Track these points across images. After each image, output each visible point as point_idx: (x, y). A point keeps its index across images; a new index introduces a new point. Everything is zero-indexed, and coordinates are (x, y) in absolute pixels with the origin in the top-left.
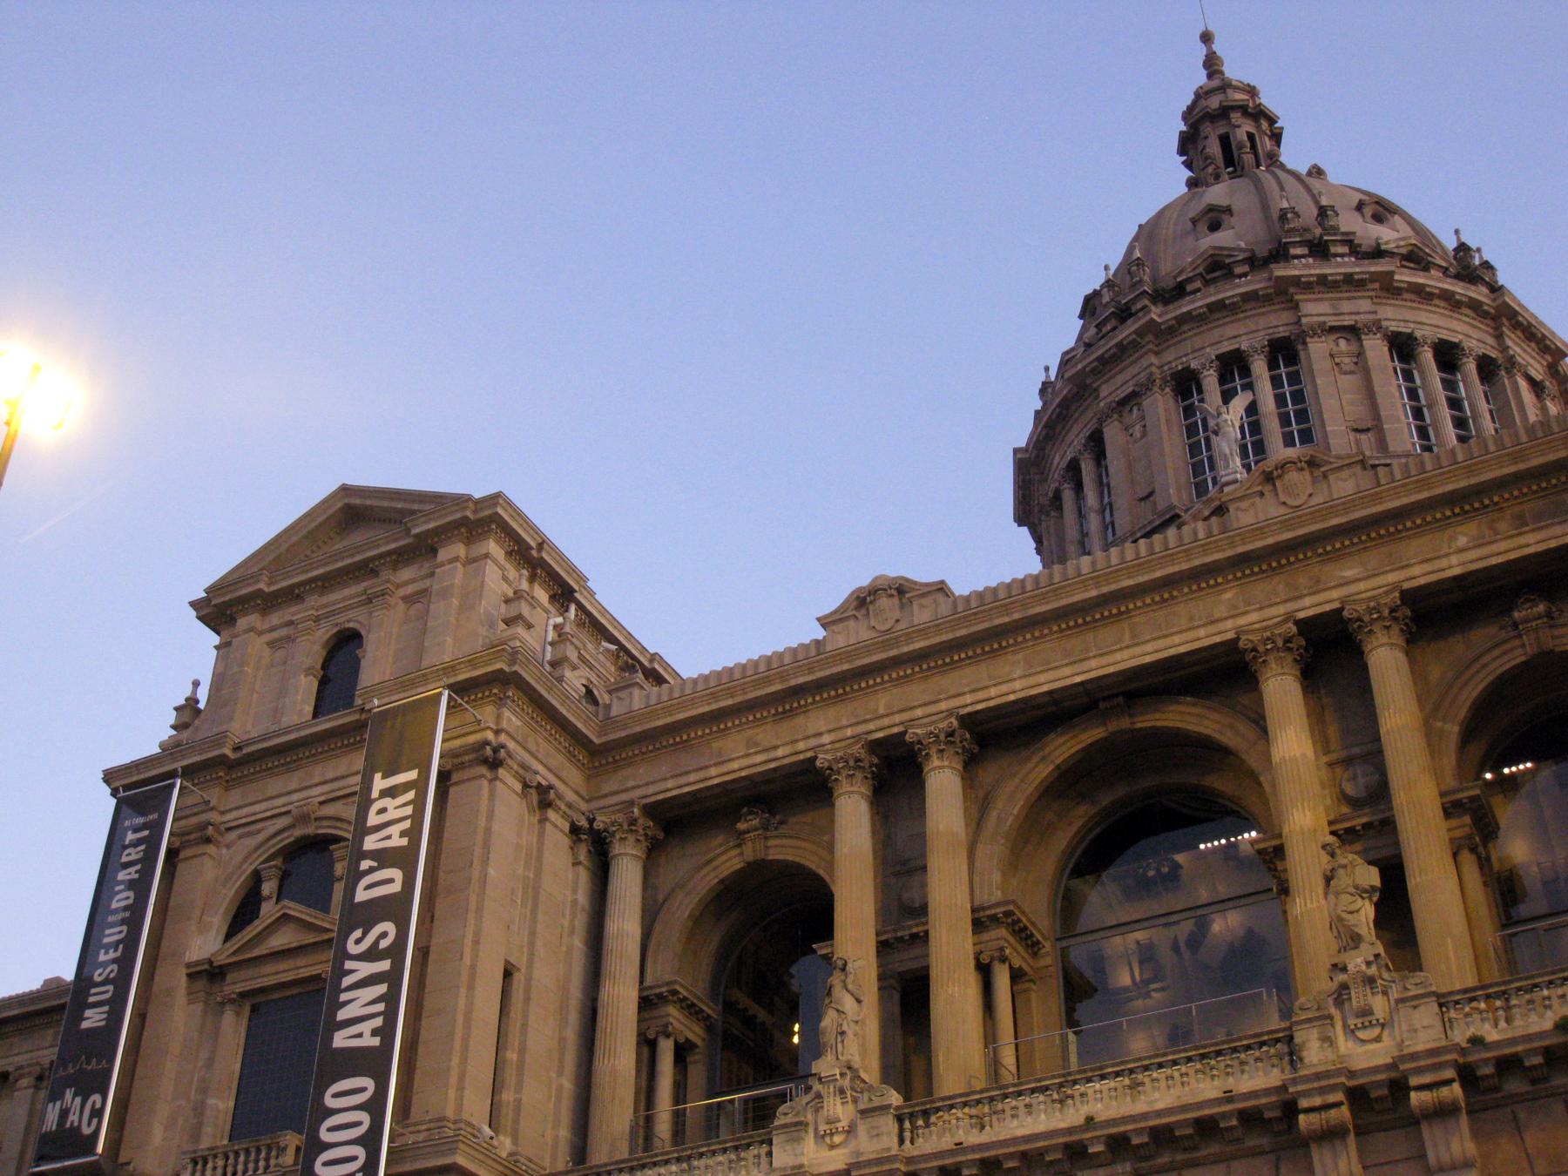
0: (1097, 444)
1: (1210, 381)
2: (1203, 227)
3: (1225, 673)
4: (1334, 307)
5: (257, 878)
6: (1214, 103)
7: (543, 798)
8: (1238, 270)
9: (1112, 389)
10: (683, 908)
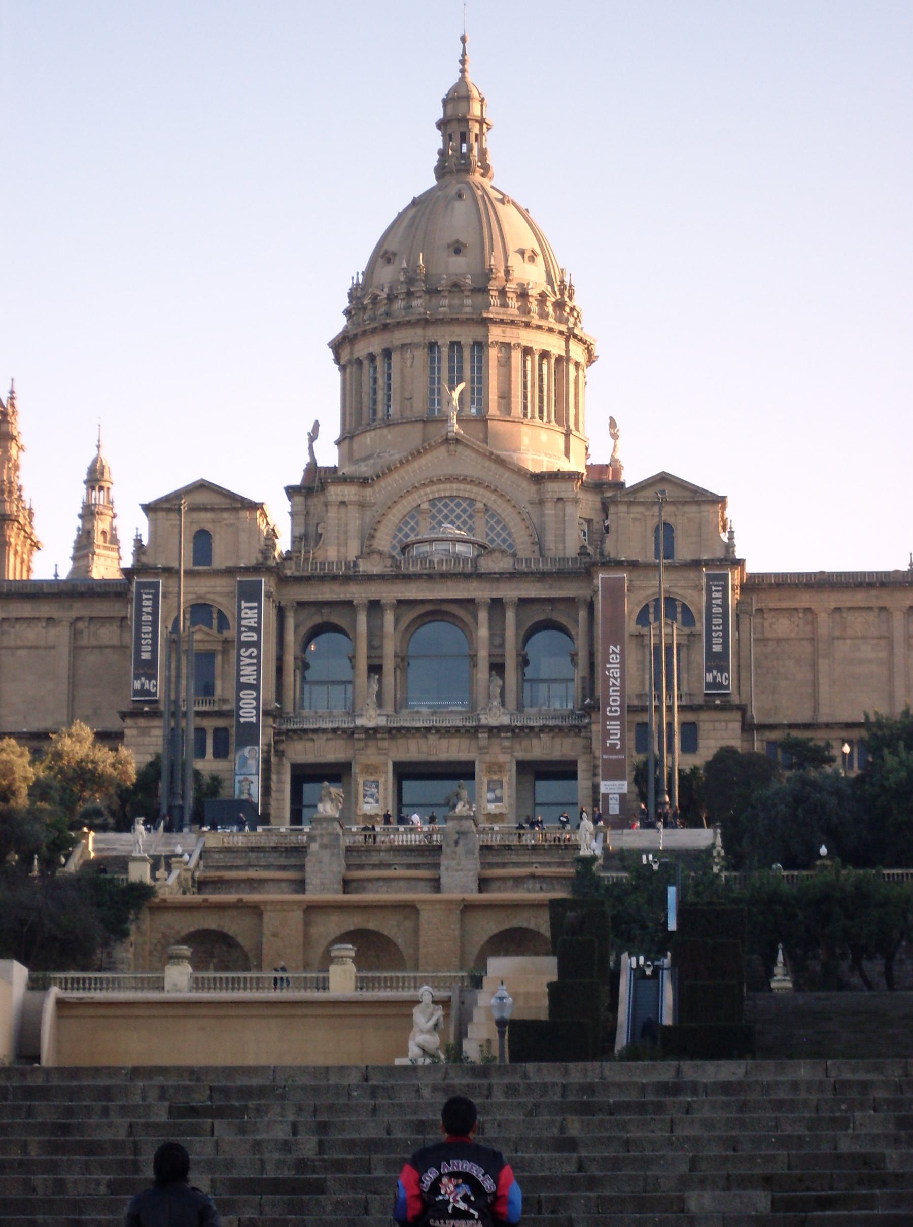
0: (387, 353)
1: (445, 351)
2: (452, 250)
3: (468, 603)
4: (504, 332)
7: (274, 601)
9: (400, 337)
10: (303, 630)
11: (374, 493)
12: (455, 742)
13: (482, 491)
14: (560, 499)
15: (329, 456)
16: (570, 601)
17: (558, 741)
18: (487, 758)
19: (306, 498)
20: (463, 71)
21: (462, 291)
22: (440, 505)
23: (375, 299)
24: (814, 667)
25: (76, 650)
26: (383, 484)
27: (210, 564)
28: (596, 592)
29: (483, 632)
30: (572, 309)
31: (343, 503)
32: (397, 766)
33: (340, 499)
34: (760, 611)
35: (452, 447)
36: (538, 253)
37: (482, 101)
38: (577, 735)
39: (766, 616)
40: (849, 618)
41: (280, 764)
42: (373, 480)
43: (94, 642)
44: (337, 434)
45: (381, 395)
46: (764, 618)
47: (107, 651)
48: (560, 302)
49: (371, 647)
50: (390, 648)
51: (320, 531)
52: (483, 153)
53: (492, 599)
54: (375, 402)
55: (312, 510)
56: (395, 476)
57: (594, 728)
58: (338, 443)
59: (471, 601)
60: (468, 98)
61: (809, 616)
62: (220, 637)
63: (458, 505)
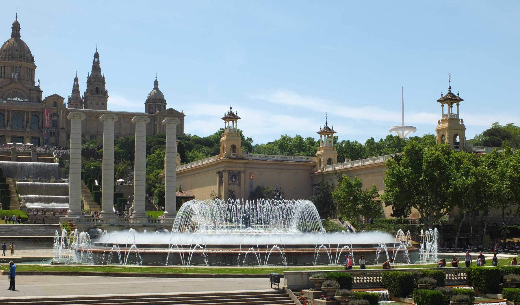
0: (4, 67)
3: (24, 112)
36: (29, 52)
45: (3, 73)
50: (10, 117)
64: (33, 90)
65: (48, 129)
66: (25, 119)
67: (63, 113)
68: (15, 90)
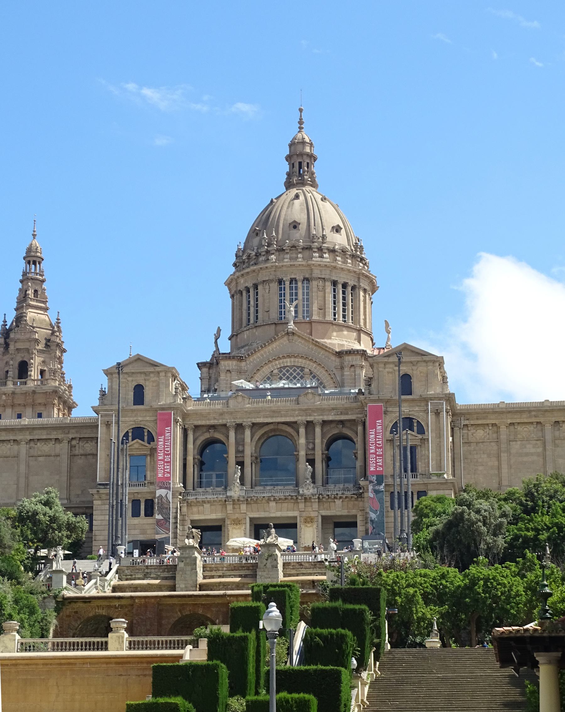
0: (256, 287)
1: (287, 283)
2: (292, 226)
3: (293, 425)
5: (127, 432)
6: (299, 149)
8: (300, 250)
10: (199, 442)
11: (246, 365)
12: (285, 505)
13: (308, 362)
14: (352, 366)
15: (225, 347)
16: (353, 421)
17: (345, 503)
18: (304, 514)
19: (209, 369)
20: (301, 128)
21: (297, 249)
22: (284, 371)
23: (249, 257)
24: (499, 458)
25: (72, 456)
26: (251, 359)
27: (143, 404)
28: (366, 416)
29: (302, 441)
30: (362, 259)
31: (229, 371)
32: (251, 519)
33: (227, 368)
34: (466, 425)
35: (291, 337)
37: (311, 145)
38: (356, 500)
39: (469, 428)
40: (519, 429)
41: (183, 520)
42: (246, 357)
43: (82, 452)
44: (229, 334)
45: (252, 310)
46: (468, 430)
47: (89, 457)
48: (356, 254)
49: (237, 451)
50: (249, 450)
51: (216, 387)
52: (313, 174)
53: (307, 422)
54: (249, 314)
55: (213, 376)
56: (259, 354)
57: (366, 495)
58: (230, 339)
59: (295, 423)
60: (303, 143)
61: (495, 428)
62: (149, 446)
63: (295, 371)
64: (351, 352)
65: (380, 479)
66: (302, 453)
67: (437, 413)
68: (288, 362)
